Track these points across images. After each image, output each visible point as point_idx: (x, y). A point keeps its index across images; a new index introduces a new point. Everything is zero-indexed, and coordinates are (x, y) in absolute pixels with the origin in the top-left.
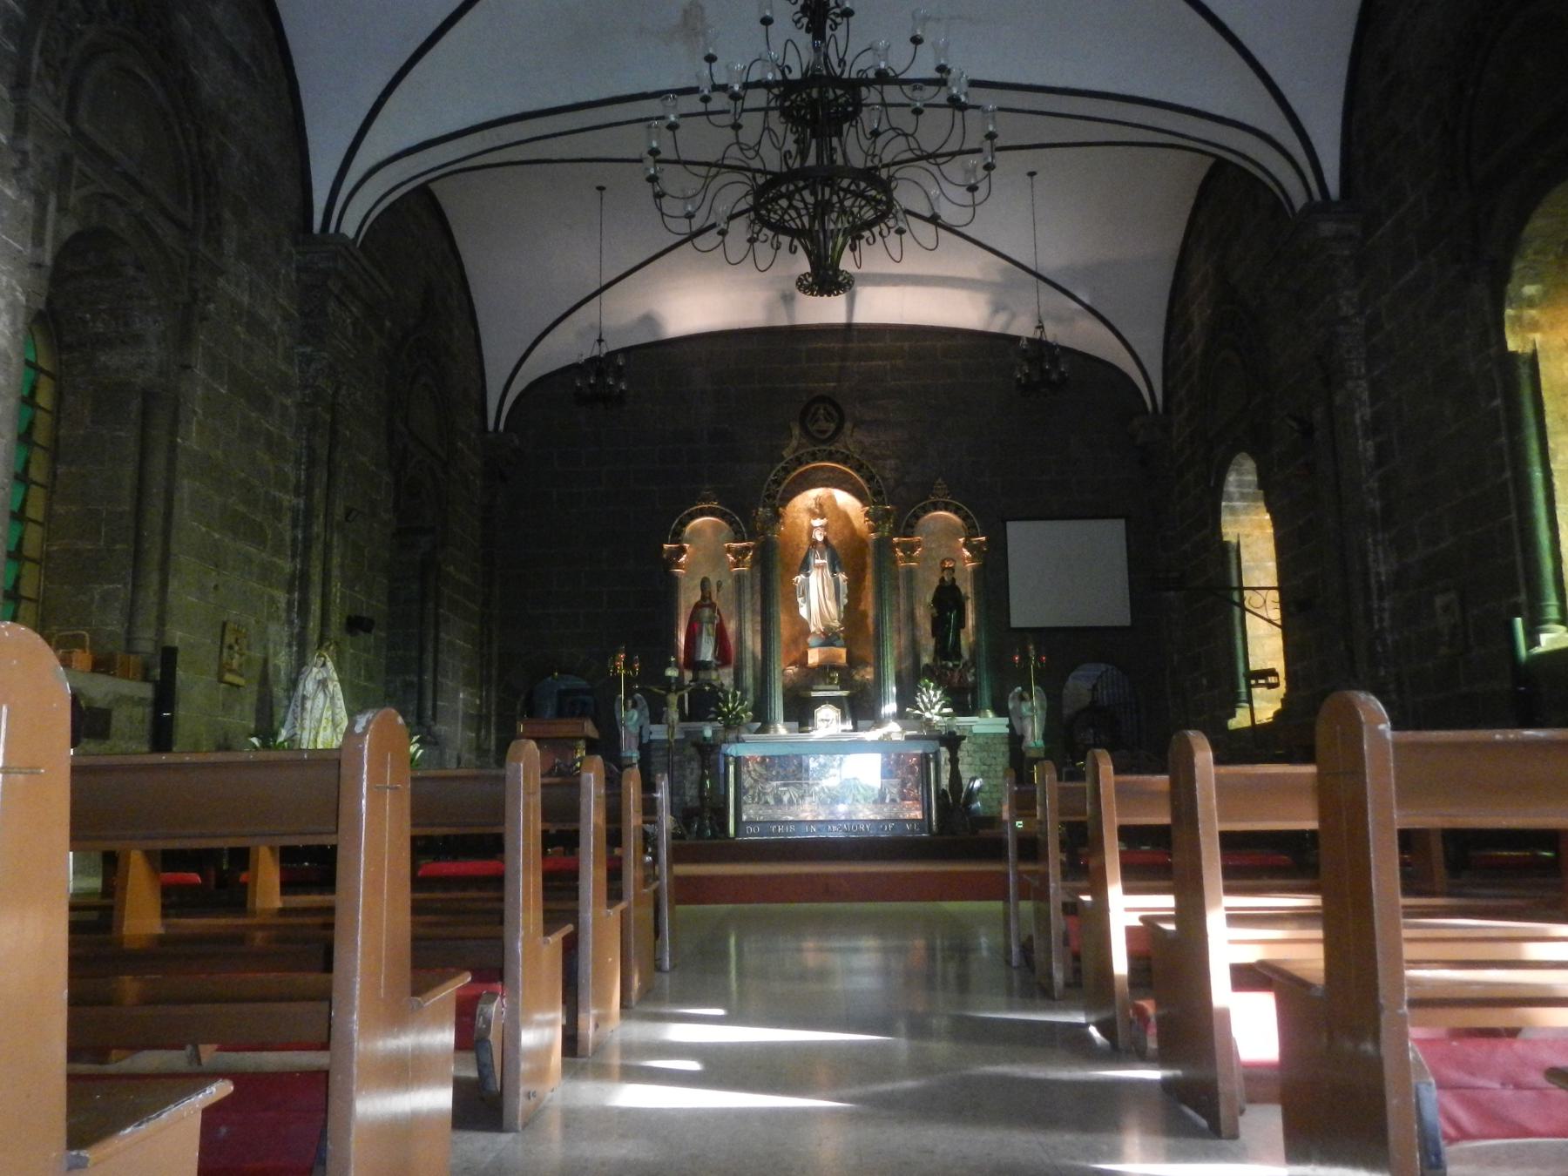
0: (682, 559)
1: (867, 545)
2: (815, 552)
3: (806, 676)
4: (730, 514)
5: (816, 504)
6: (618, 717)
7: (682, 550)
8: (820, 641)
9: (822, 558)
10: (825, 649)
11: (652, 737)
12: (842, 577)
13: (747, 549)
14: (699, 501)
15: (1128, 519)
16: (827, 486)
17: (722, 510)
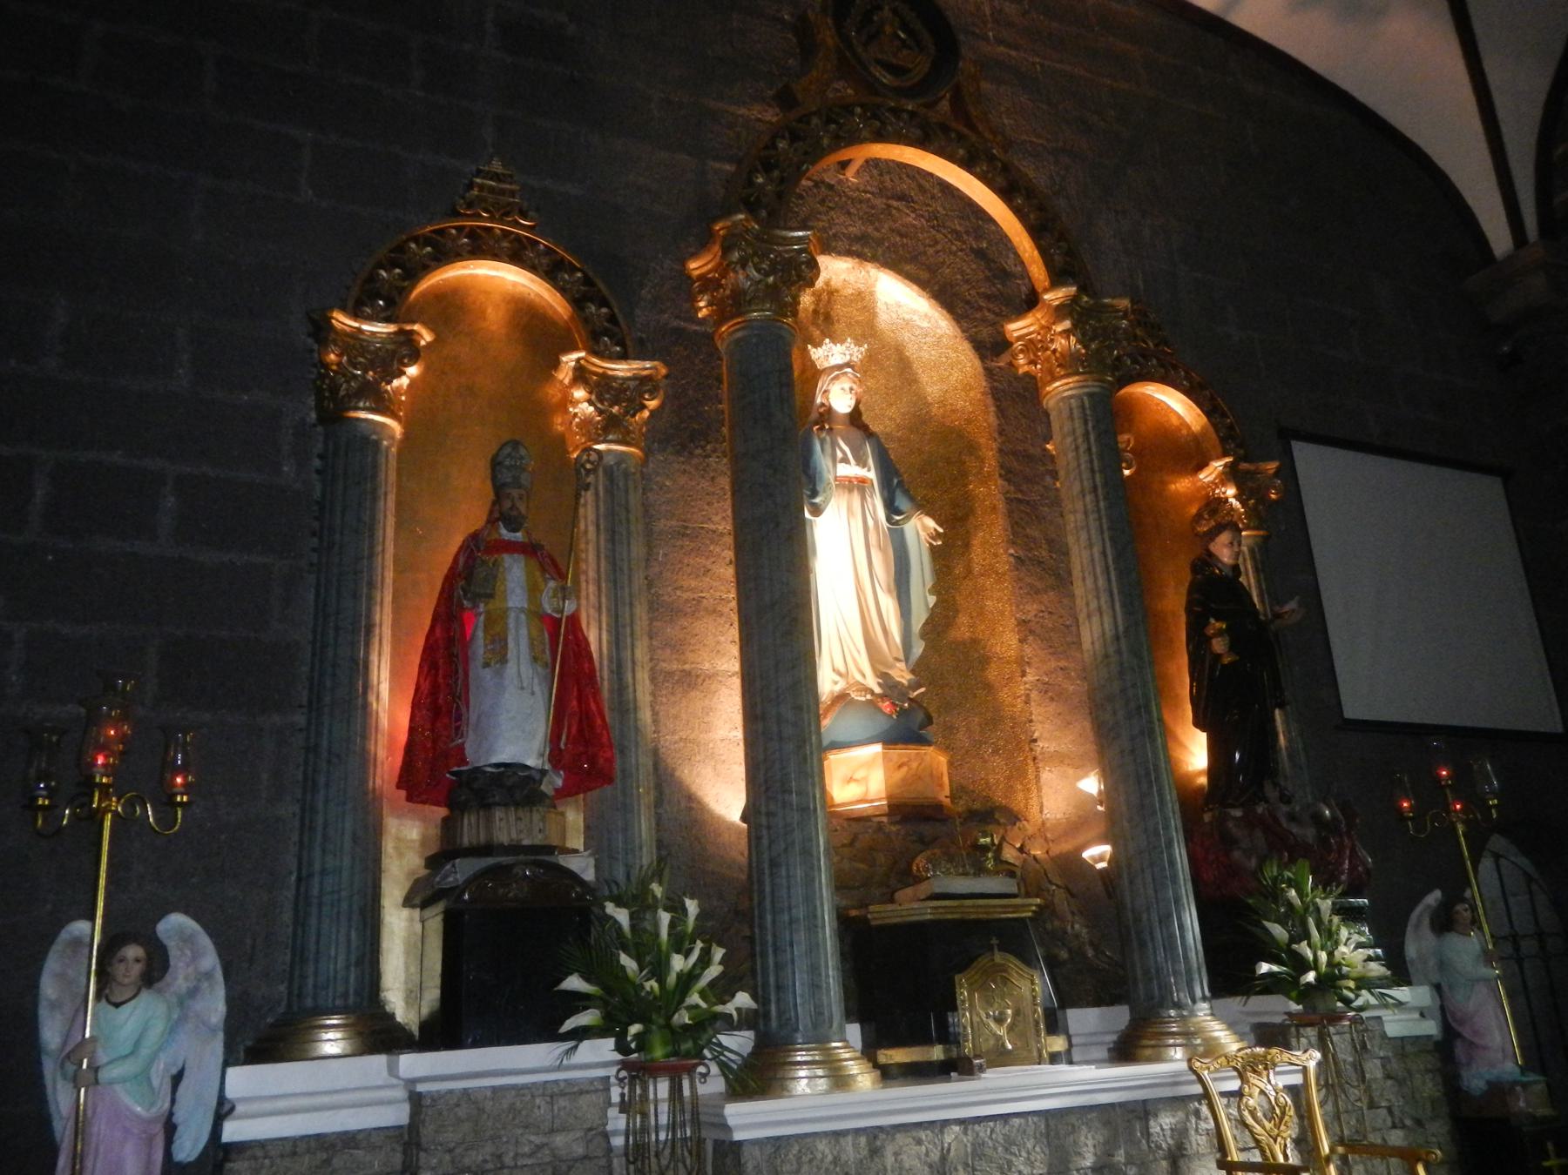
0: (403, 382)
1: (972, 448)
2: (834, 445)
3: (851, 844)
4: (573, 269)
5: (815, 312)
6: (51, 1034)
7: (406, 348)
8: (881, 724)
9: (861, 462)
10: (898, 753)
11: (232, 1131)
12: (921, 528)
13: (644, 384)
14: (470, 205)
15: (1506, 475)
16: (861, 256)
17: (549, 251)
